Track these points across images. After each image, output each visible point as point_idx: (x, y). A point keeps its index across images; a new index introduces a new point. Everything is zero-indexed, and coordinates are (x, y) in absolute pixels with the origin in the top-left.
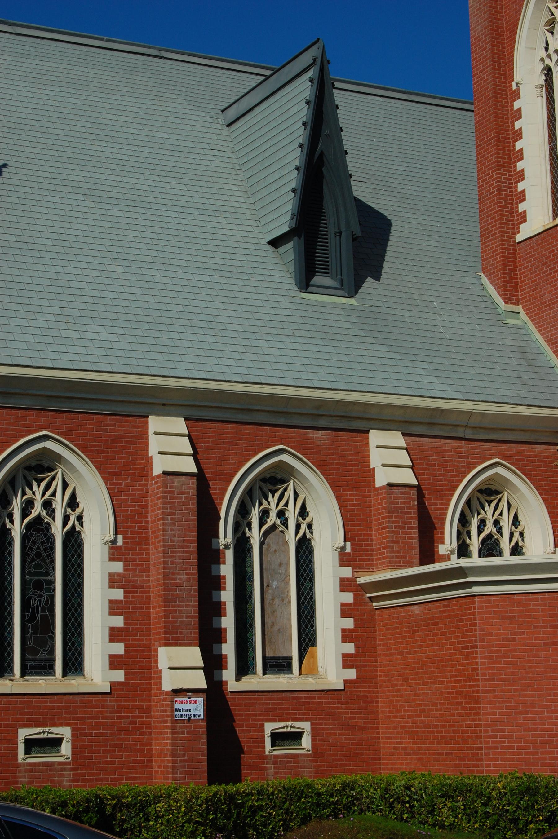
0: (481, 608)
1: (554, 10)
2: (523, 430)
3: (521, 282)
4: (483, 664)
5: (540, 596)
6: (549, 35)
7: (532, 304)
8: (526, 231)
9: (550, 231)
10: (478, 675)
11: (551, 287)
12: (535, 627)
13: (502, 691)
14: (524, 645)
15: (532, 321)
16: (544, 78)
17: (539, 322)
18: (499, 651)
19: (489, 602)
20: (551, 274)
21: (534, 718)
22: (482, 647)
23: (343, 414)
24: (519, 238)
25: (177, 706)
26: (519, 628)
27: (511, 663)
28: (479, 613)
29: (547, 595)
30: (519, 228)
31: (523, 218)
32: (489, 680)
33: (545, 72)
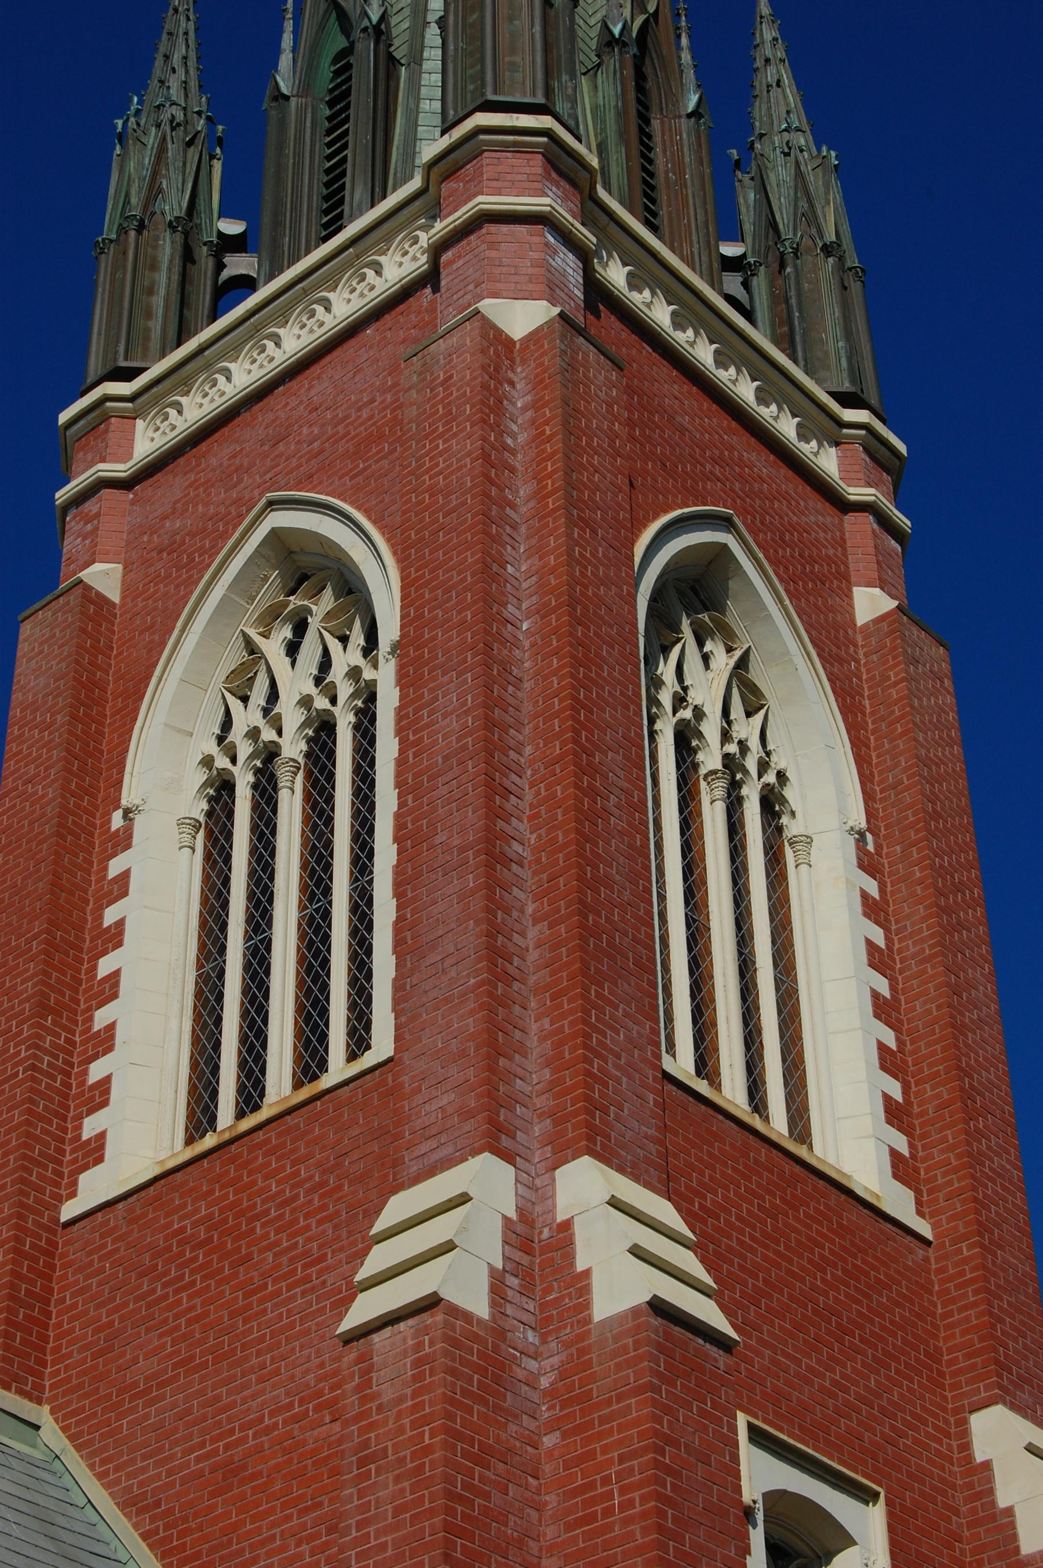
3: (58, 1337)
6: (235, 704)
7: (86, 1396)
9: (179, 1175)
11: (161, 1336)
15: (78, 1448)
16: (204, 806)
20: (165, 1297)
24: (69, 1210)
30: (74, 1183)
31: (94, 1152)
33: (212, 792)
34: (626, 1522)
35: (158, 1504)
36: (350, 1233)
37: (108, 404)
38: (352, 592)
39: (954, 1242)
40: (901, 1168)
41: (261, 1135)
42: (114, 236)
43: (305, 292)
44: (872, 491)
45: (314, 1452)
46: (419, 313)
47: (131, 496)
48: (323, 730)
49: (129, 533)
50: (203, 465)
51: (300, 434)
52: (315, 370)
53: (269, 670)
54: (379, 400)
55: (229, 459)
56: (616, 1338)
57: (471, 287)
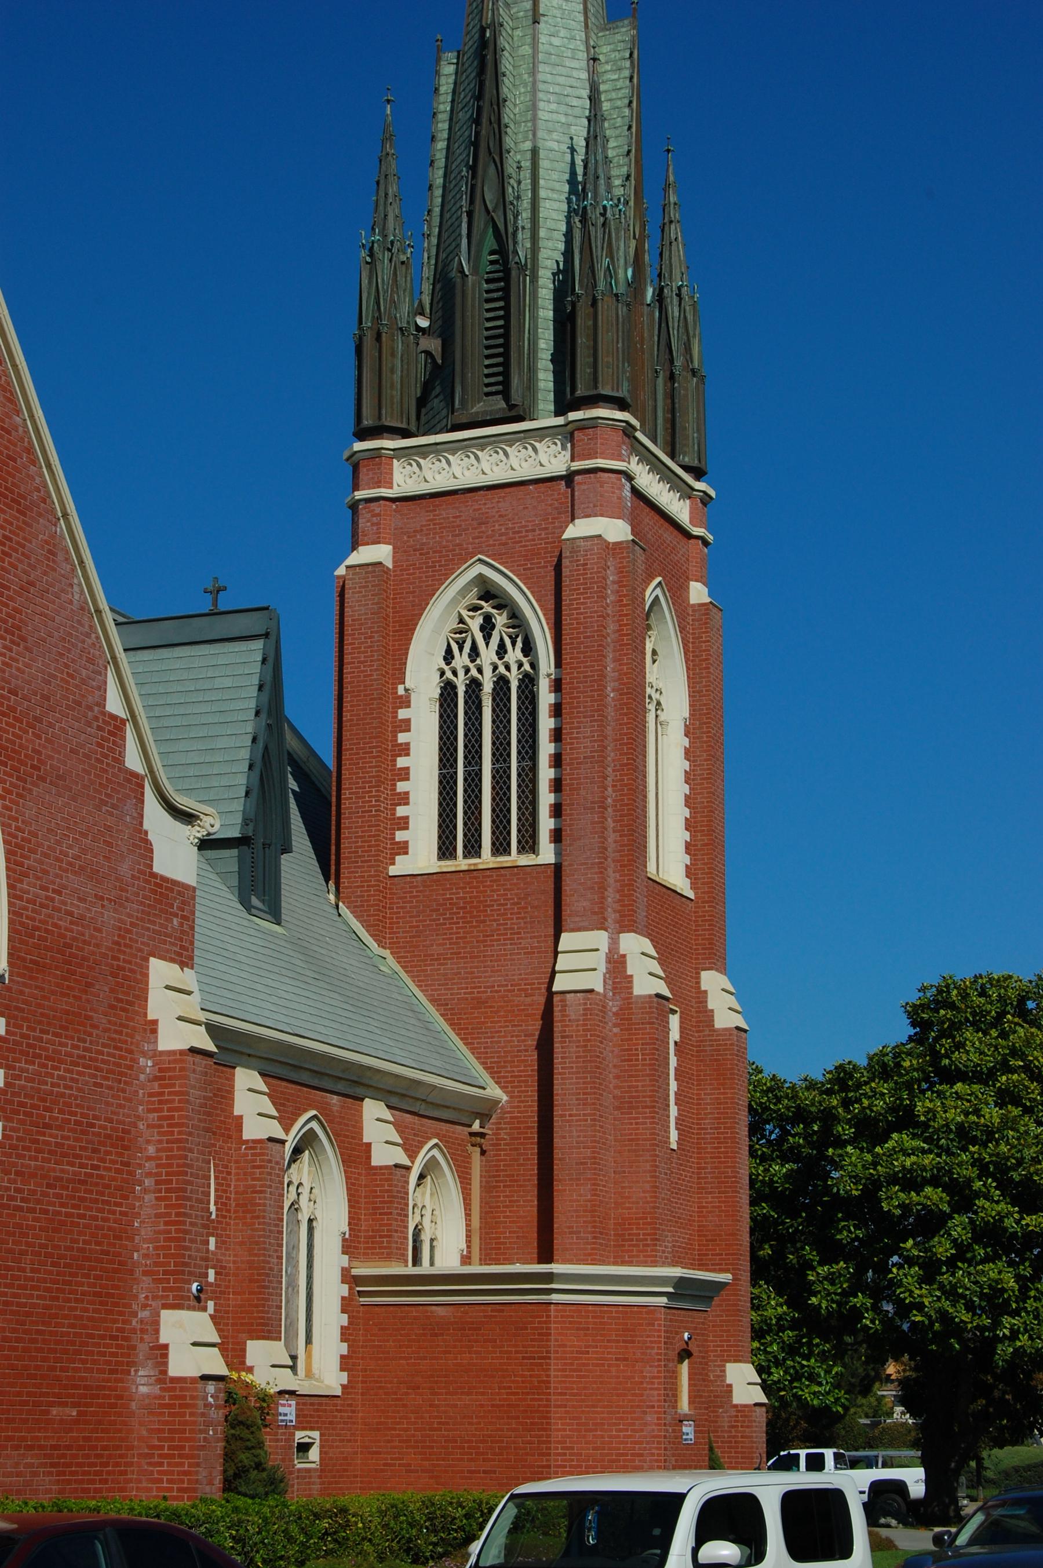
0: (556, 1317)
1: (467, 619)
2: (454, 1109)
4: (556, 1376)
5: (614, 1309)
6: (455, 647)
7: (408, 952)
8: (401, 866)
10: (549, 1388)
12: (609, 1341)
13: (573, 1406)
14: (596, 1359)
17: (418, 976)
18: (572, 1364)
19: (565, 1311)
21: (602, 1437)
22: (556, 1358)
23: (355, 1079)
24: (393, 871)
25: (281, 1410)
26: (593, 1340)
27: (584, 1377)
28: (555, 1323)
29: (621, 1309)
30: (394, 859)
31: (403, 848)
32: (561, 1394)
34: (643, 1065)
35: (447, 1005)
36: (532, 928)
38: (517, 620)
39: (703, 902)
40: (689, 872)
41: (488, 873)
42: (370, 324)
43: (495, 442)
44: (703, 530)
45: (517, 1006)
48: (502, 684)
52: (502, 492)
53: (472, 635)
54: (538, 532)
56: (642, 1003)
57: (591, 505)
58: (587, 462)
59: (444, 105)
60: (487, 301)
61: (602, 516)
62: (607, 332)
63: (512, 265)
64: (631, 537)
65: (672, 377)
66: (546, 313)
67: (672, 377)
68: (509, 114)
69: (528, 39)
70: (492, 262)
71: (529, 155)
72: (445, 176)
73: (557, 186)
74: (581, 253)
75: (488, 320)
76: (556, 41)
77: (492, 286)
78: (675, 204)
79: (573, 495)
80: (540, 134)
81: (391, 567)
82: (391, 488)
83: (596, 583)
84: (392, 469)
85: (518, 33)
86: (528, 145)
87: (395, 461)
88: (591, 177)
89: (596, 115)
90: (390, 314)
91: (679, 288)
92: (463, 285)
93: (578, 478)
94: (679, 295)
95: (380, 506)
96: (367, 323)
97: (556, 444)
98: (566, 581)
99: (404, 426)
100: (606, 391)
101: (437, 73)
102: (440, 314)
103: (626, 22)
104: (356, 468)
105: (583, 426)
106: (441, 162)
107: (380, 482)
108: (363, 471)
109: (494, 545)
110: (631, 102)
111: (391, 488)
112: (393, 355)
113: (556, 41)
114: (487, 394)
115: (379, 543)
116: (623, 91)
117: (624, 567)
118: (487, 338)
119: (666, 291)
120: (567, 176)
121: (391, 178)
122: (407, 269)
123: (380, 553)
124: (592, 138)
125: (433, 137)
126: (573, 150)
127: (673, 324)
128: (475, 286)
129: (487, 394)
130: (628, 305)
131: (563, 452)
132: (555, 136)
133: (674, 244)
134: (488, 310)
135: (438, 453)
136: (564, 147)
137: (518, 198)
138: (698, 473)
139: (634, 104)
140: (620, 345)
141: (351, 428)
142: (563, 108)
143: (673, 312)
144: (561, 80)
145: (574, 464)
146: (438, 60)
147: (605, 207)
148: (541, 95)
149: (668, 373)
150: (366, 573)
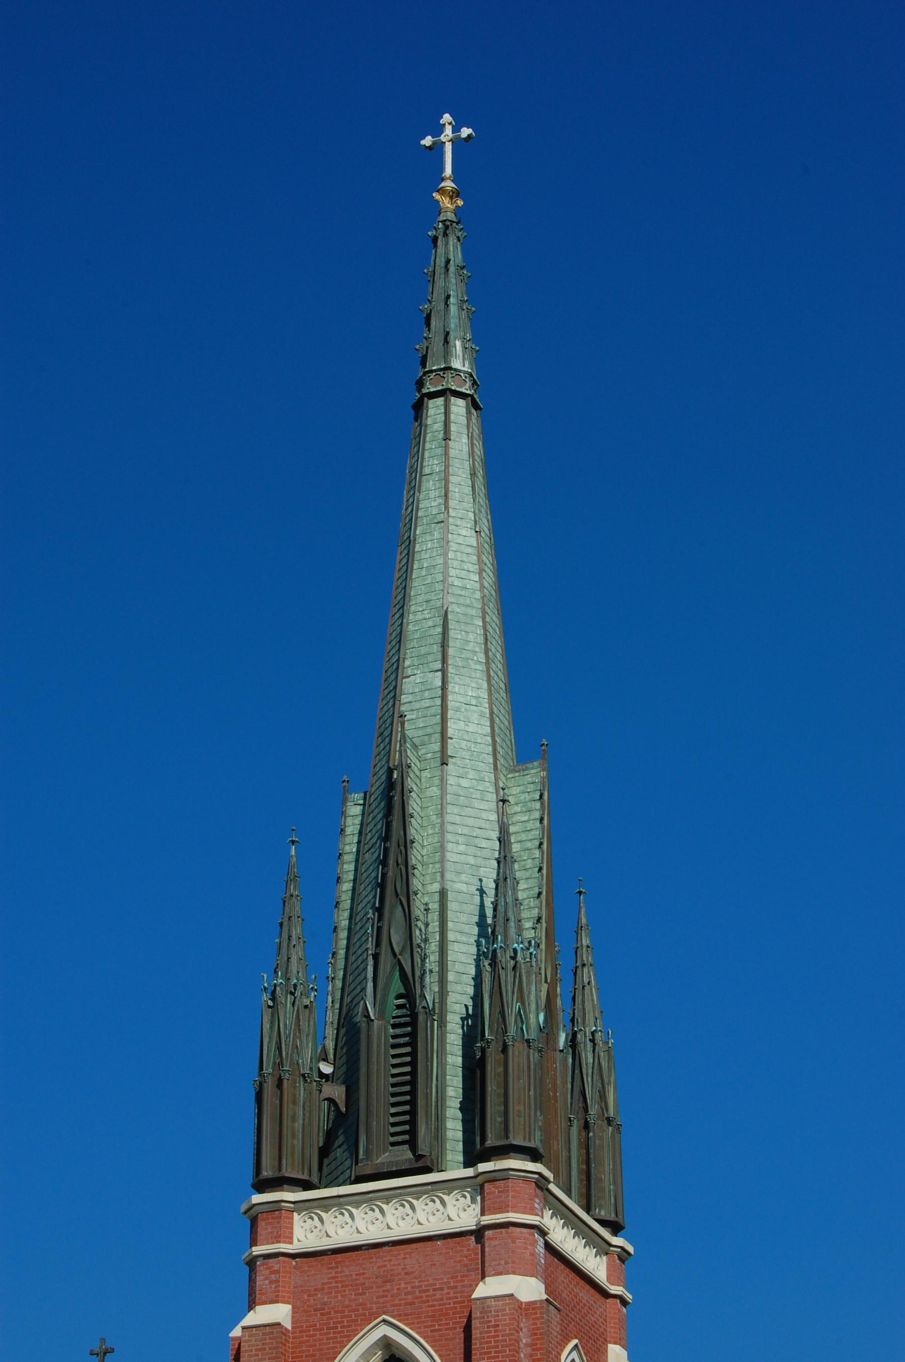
37: (283, 1204)
43: (401, 1195)
44: (621, 1288)
46: (468, 1250)
47: (294, 1263)
49: (295, 1287)
50: (339, 1270)
51: (400, 1284)
54: (446, 1291)
55: (357, 1275)
57: (503, 1262)
58: (498, 1216)
59: (350, 846)
60: (394, 1046)
61: (514, 1273)
62: (519, 1078)
63: (419, 1009)
64: (545, 1297)
65: (586, 1126)
66: (455, 1059)
67: (586, 1126)
68: (415, 857)
69: (436, 781)
70: (399, 1007)
71: (437, 897)
72: (351, 918)
73: (466, 928)
74: (491, 997)
75: (394, 1066)
76: (465, 783)
77: (398, 1031)
78: (588, 947)
79: (483, 1252)
80: (448, 876)
81: (289, 1327)
82: (291, 1243)
83: (507, 1346)
84: (292, 1223)
85: (426, 774)
86: (436, 887)
87: (295, 1214)
88: (501, 920)
89: (505, 857)
90: (292, 1059)
91: (593, 1033)
92: (368, 1031)
93: (488, 1233)
94: (593, 1041)
95: (279, 1262)
96: (268, 1069)
97: (465, 1197)
98: (476, 1344)
99: (305, 1177)
100: (518, 1141)
101: (343, 814)
102: (344, 1059)
103: (536, 764)
104: (254, 1221)
105: (493, 1178)
106: (346, 904)
107: (280, 1236)
108: (261, 1224)
109: (400, 1305)
110: (541, 844)
111: (291, 1243)
112: (294, 1102)
113: (465, 783)
114: (393, 1144)
115: (277, 1302)
116: (533, 832)
117: (538, 1329)
118: (393, 1085)
119: (579, 1036)
120: (476, 919)
121: (294, 920)
122: (310, 1013)
123: (277, 1313)
124: (502, 879)
125: (339, 878)
126: (482, 892)
127: (587, 1071)
128: (381, 1032)
129: (393, 1144)
130: (540, 1051)
131: (473, 1206)
132: (463, 877)
133: (587, 987)
134: (394, 1056)
135: (340, 1206)
136: (473, 889)
137: (426, 940)
138: (616, 1228)
139: (545, 846)
140: (532, 1093)
141: (249, 1178)
142: (472, 850)
143: (586, 1058)
144: (471, 821)
145: (484, 1218)
146: (344, 801)
147: (515, 950)
148: (449, 837)
149: (583, 1121)
150: (264, 1334)
